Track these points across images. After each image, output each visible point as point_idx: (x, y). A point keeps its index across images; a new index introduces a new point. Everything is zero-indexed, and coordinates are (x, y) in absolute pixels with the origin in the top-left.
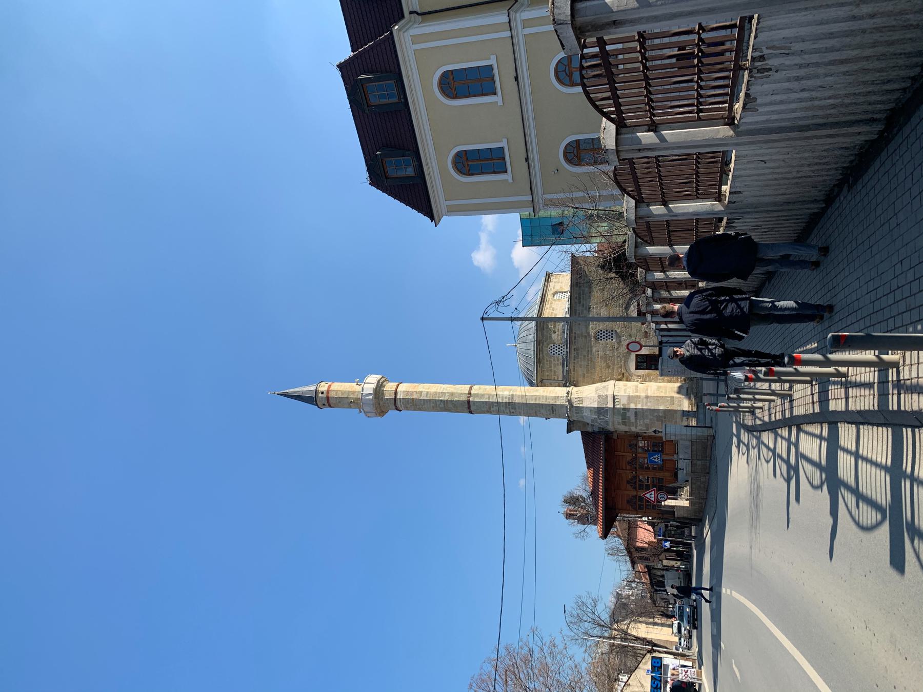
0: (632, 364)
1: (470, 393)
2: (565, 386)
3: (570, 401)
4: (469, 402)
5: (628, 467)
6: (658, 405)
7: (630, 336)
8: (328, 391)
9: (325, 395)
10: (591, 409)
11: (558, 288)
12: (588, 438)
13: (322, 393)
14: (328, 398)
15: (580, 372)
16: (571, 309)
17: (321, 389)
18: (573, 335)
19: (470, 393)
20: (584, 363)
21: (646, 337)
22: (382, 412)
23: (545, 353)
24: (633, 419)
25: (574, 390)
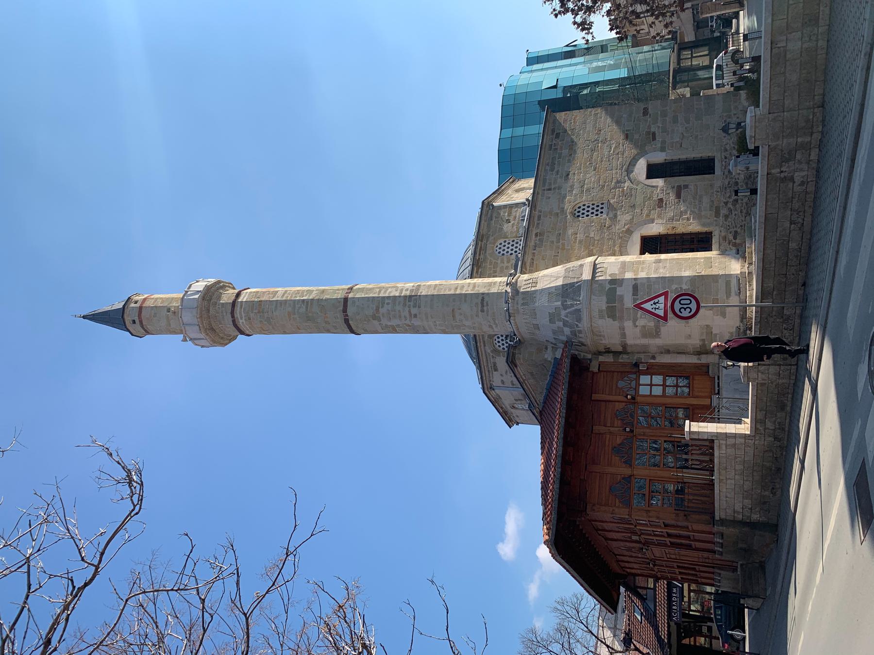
1: (351, 288)
3: (514, 286)
6: (680, 270)
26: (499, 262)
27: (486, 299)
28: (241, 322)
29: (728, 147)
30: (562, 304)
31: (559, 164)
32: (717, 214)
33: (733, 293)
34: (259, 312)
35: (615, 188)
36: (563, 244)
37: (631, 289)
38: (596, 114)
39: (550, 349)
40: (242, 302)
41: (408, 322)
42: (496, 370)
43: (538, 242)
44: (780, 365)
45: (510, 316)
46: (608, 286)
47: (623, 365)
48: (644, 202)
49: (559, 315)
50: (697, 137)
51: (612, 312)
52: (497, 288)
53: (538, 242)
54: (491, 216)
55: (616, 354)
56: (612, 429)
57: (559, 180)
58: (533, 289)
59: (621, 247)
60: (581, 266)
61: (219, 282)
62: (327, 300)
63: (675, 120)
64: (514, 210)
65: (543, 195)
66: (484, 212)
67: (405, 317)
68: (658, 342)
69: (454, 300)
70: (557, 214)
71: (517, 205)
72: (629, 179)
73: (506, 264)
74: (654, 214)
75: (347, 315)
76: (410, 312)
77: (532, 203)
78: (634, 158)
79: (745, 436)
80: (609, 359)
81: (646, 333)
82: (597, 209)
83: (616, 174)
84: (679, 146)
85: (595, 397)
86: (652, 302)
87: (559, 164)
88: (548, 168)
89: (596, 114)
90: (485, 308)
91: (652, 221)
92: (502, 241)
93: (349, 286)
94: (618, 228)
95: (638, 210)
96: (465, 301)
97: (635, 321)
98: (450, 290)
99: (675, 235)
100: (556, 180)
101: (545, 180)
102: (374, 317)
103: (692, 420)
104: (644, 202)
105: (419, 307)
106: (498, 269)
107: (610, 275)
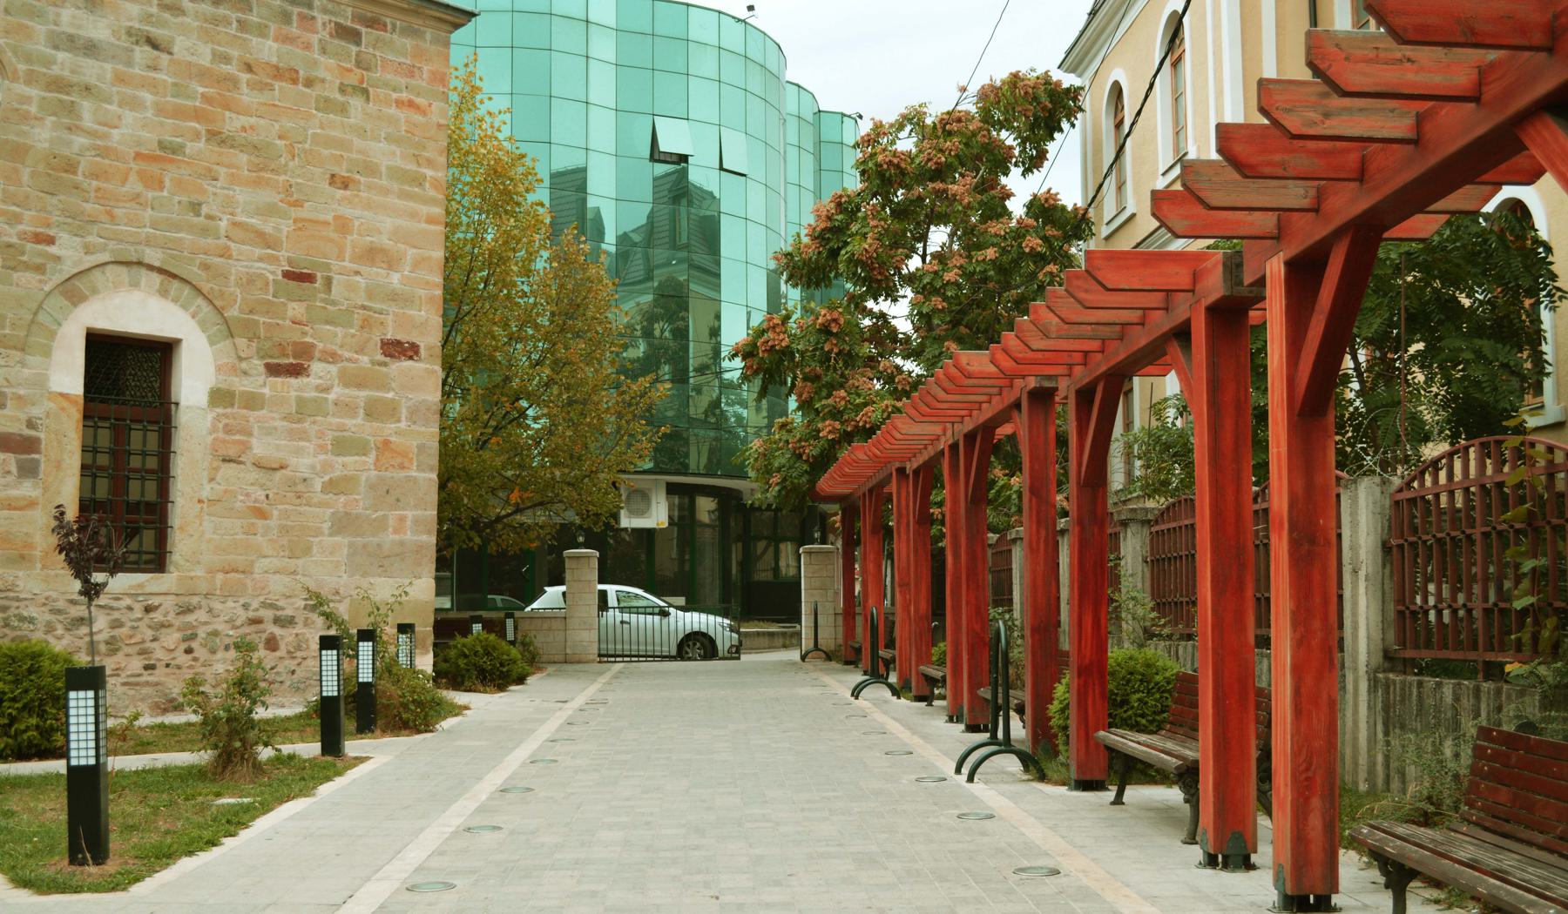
29: (201, 615)
31: (216, 21)
50: (261, 514)
63: (343, 446)
84: (232, 452)
87: (216, 21)
89: (419, 180)
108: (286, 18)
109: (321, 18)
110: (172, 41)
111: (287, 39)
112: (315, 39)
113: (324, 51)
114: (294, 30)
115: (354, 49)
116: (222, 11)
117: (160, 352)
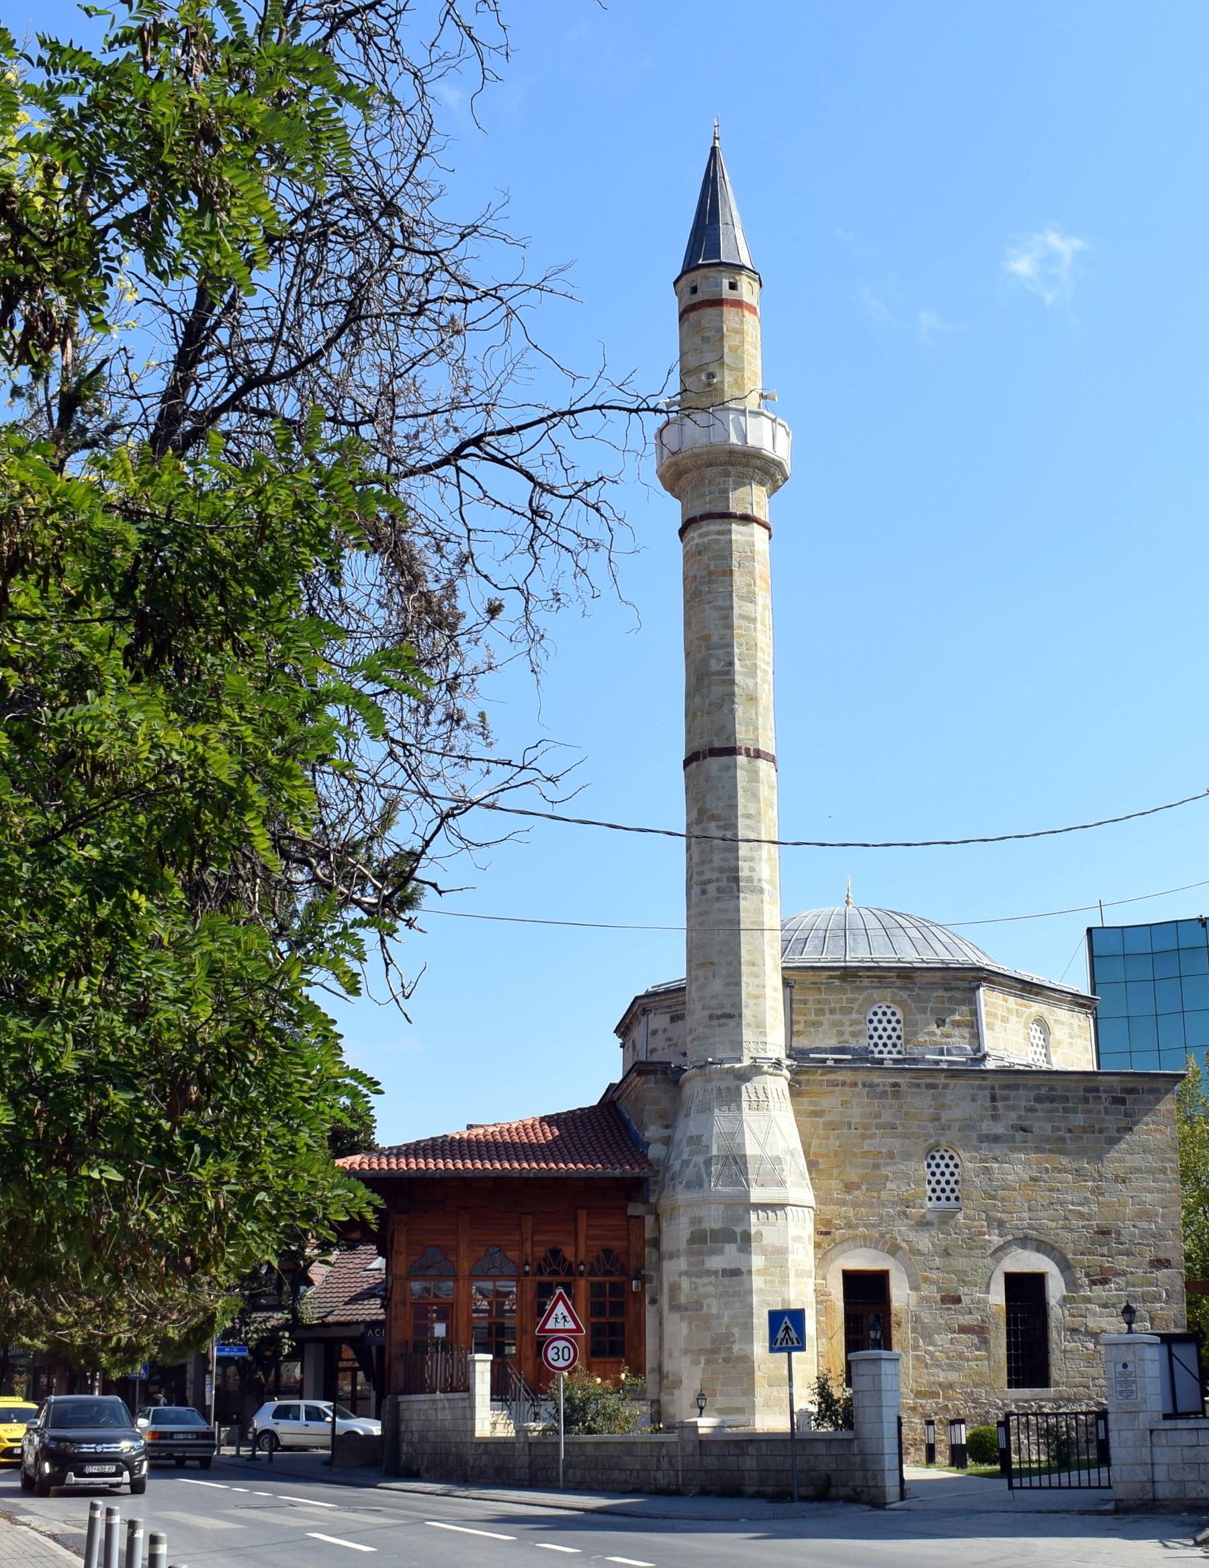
0: (863, 1261)
1: (758, 754)
2: (793, 1053)
3: (755, 1070)
4: (732, 751)
5: (541, 1251)
7: (947, 1253)
8: (739, 304)
9: (727, 293)
10: (735, 1135)
11: (1059, 1033)
12: (604, 1126)
13: (733, 286)
14: (718, 302)
15: (826, 1103)
16: (1013, 1077)
17: (744, 281)
18: (941, 1080)
19: (758, 754)
20: (856, 1114)
21: (944, 1300)
22: (678, 475)
23: (876, 994)
24: (716, 1263)
25: (777, 1085)
26: (854, 1016)
27: (731, 1022)
28: (693, 534)
30: (711, 1158)
32: (919, 1394)
33: (725, 1418)
34: (710, 574)
35: (989, 1219)
36: (872, 1137)
37: (733, 1266)
38: (1164, 1171)
39: (666, 1132)
40: (730, 532)
41: (695, 878)
42: (674, 1019)
43: (878, 1090)
44: (530, 1467)
45: (701, 1067)
46: (738, 1230)
47: (641, 1256)
48: (955, 1272)
49: (698, 1153)
51: (703, 1240)
52: (751, 1039)
53: (878, 1090)
54: (952, 989)
55: (656, 1243)
56: (529, 1243)
57: (1013, 1115)
58: (745, 1105)
59: (865, 1237)
60: (782, 1183)
61: (779, 465)
62: (732, 712)
64: (966, 1032)
65: (980, 1087)
66: (959, 974)
67: (701, 873)
68: (666, 1307)
69: (729, 964)
70: (937, 1119)
71: (976, 1036)
72: (1008, 1243)
73: (848, 1029)
74: (928, 1291)
75: (705, 757)
76: (710, 881)
77: (973, 1070)
78: (1053, 1248)
79: (473, 1431)
80: (648, 1235)
81: (675, 1288)
82: (950, 1194)
83: (1020, 1219)
85: (583, 1216)
86: (566, 1313)
88: (1043, 1091)
90: (715, 1022)
91: (915, 1288)
92: (899, 1016)
93: (767, 744)
94: (902, 1231)
95: (938, 1262)
96: (728, 985)
97: (687, 1273)
98: (749, 952)
99: (890, 1326)
100: (1013, 1108)
101: (1016, 1087)
102: (702, 812)
103: (492, 1362)
104: (955, 1272)
105: (718, 899)
106: (838, 1017)
107: (760, 1234)
108: (1086, 1100)
109: (1104, 1096)
110: (1032, 1126)
111: (1089, 1111)
112: (1102, 1107)
113: (1107, 1113)
114: (1091, 1106)
115: (1123, 1107)
116: (1054, 1105)
117: (1037, 1281)
